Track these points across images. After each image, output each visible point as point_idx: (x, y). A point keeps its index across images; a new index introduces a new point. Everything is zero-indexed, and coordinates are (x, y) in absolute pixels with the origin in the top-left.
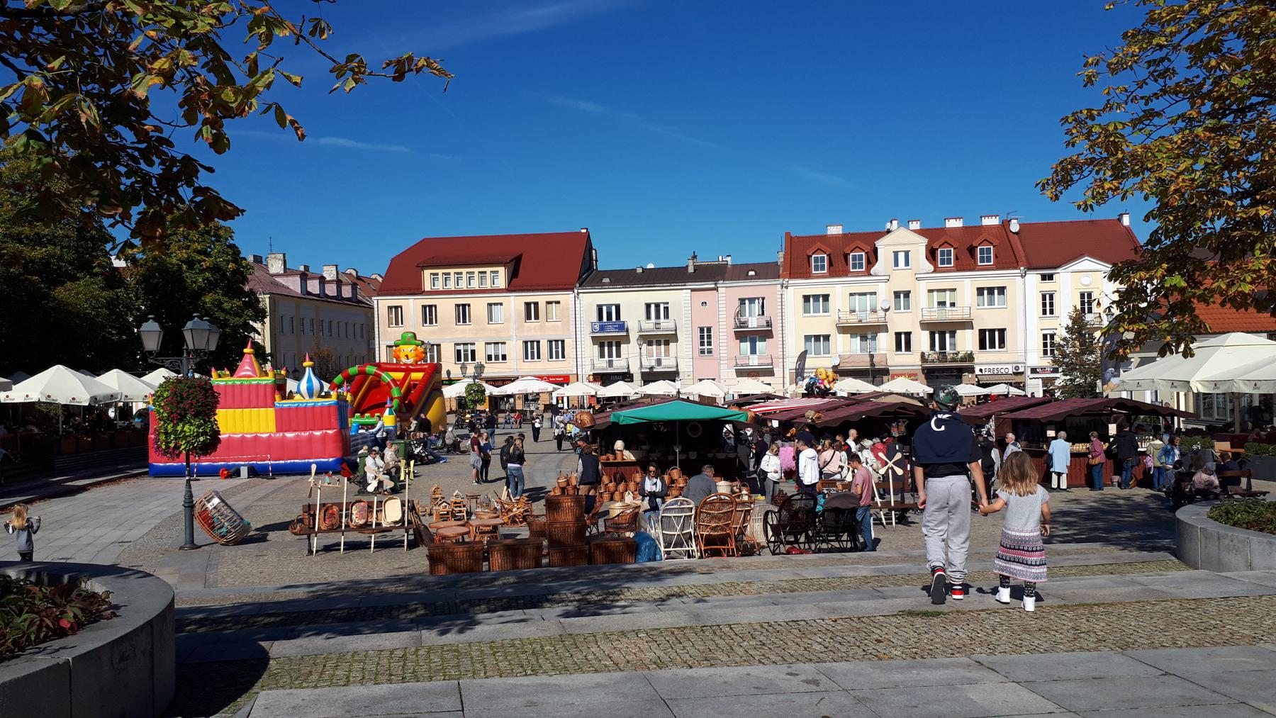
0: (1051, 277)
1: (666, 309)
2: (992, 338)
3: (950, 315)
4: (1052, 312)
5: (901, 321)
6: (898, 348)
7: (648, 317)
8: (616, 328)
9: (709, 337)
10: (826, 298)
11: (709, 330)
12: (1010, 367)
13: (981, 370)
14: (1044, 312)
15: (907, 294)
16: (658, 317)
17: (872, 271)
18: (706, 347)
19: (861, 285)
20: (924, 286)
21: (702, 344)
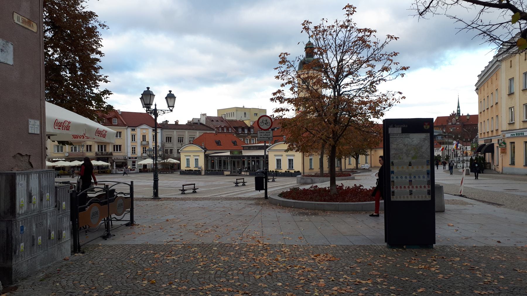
0: (134, 130)
2: (118, 148)
4: (134, 140)
6: (87, 151)
12: (123, 157)
13: (114, 158)
14: (132, 140)
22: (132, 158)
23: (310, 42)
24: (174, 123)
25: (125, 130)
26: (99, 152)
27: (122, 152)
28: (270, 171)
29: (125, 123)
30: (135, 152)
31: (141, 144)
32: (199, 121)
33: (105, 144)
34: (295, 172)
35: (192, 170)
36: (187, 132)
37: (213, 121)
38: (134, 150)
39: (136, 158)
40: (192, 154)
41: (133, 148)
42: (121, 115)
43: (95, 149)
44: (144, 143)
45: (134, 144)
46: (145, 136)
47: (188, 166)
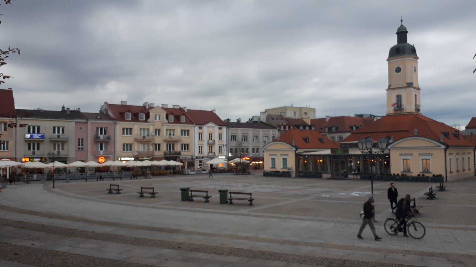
1: (63, 130)
3: (173, 138)
4: (201, 139)
5: (158, 140)
7: (54, 132)
8: (39, 137)
9: (79, 142)
10: (131, 129)
11: (82, 140)
12: (190, 157)
13: (182, 158)
15: (159, 130)
16: (59, 132)
17: (149, 120)
18: (81, 147)
19: (144, 125)
20: (165, 128)
21: (79, 145)
22: (199, 157)
23: (402, 26)
24: (236, 121)
25: (193, 128)
26: (167, 151)
27: (189, 151)
28: (394, 174)
29: (193, 121)
30: (201, 152)
31: (208, 143)
32: (259, 119)
33: (173, 143)
34: (434, 175)
35: (279, 172)
36: (250, 130)
37: (273, 119)
38: (201, 148)
39: (203, 158)
40: (278, 154)
41: (200, 147)
42: (187, 112)
43: (164, 148)
44: (211, 142)
45: (201, 143)
46: (211, 134)
47: (274, 166)
